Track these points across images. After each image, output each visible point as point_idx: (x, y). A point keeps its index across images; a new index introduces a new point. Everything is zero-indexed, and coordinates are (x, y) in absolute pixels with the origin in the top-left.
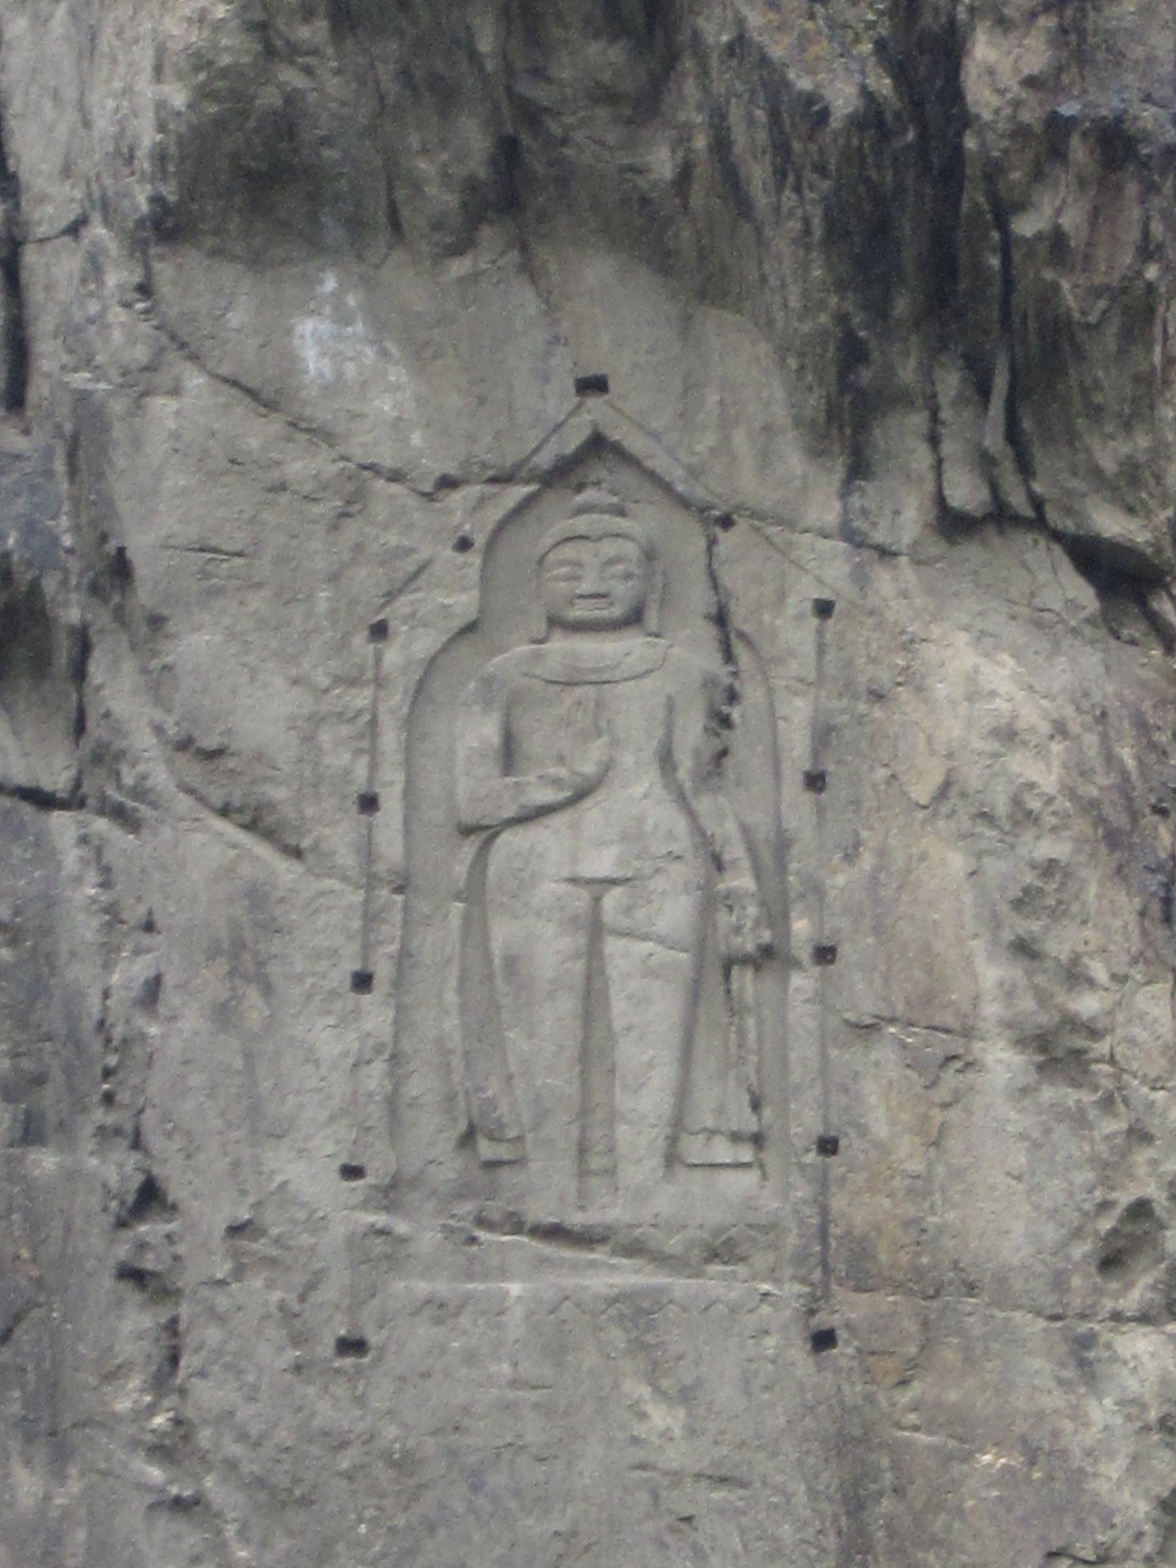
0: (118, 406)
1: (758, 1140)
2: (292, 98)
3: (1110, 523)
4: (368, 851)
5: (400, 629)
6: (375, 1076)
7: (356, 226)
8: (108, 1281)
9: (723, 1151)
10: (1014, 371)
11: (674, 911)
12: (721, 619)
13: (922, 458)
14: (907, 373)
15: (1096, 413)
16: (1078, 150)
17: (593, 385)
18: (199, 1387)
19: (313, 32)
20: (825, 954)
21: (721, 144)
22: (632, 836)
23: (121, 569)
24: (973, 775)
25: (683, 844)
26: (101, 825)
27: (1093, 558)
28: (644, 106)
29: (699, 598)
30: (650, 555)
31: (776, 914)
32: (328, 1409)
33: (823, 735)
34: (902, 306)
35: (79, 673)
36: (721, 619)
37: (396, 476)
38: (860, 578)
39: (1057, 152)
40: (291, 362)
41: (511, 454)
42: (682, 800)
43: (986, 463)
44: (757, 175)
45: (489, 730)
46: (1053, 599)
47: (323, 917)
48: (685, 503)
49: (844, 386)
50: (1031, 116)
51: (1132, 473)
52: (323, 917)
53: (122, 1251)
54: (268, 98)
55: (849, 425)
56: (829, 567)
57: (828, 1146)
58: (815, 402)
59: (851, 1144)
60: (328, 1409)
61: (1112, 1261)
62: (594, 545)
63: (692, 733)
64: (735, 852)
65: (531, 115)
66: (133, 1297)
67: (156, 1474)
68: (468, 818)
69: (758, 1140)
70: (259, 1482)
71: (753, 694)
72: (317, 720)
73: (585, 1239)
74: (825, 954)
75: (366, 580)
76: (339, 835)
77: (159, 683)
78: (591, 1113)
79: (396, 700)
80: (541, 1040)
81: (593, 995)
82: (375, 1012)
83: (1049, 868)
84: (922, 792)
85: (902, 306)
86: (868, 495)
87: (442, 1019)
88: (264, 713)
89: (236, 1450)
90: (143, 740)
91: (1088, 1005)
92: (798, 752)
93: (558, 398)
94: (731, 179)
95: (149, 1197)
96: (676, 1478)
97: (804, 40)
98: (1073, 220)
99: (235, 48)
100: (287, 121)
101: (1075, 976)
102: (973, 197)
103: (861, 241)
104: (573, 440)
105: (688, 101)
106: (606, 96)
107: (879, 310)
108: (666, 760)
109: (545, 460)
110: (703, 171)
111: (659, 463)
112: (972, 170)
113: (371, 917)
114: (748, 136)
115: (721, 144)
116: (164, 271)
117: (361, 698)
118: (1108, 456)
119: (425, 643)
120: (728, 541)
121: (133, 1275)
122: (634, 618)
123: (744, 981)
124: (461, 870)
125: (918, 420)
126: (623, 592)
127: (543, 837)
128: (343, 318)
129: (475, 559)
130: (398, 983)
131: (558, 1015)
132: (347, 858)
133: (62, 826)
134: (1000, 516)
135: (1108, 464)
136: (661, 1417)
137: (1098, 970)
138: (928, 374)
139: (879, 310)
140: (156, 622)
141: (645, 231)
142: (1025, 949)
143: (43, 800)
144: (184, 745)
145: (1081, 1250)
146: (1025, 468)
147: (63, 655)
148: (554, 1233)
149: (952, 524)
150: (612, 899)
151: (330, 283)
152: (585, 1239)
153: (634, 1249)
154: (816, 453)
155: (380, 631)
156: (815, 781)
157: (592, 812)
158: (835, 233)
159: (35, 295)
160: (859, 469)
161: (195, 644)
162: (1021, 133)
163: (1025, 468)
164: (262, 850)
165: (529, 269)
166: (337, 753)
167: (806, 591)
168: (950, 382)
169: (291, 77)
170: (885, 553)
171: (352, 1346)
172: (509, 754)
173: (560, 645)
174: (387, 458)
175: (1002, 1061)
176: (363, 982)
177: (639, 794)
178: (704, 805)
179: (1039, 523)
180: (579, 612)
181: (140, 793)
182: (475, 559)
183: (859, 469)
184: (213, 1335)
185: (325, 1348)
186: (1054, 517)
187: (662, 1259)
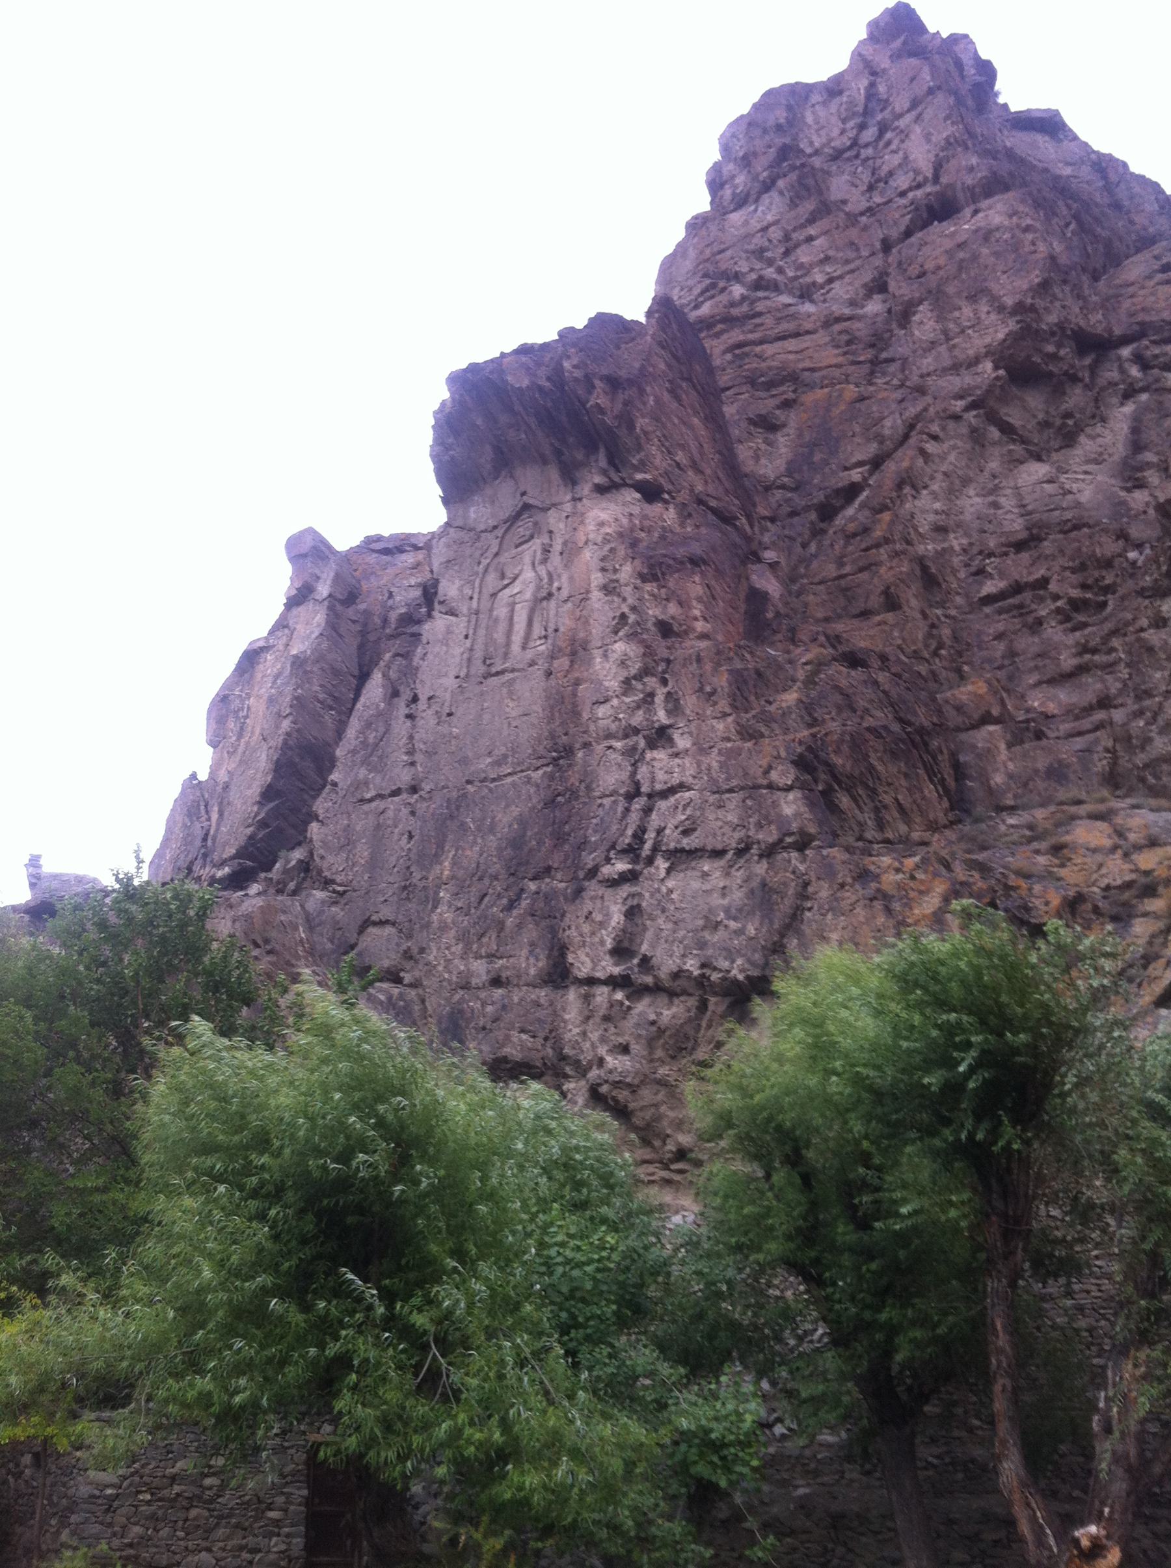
1: (546, 637)
3: (639, 476)
6: (466, 656)
8: (402, 719)
10: (607, 448)
11: (528, 595)
17: (523, 494)
20: (559, 589)
27: (640, 487)
32: (443, 729)
37: (485, 531)
38: (575, 507)
43: (604, 472)
46: (629, 499)
49: (560, 462)
51: (642, 462)
55: (570, 477)
56: (568, 507)
57: (556, 630)
60: (443, 729)
63: (539, 556)
69: (546, 637)
78: (508, 644)
81: (511, 619)
82: (468, 643)
85: (571, 440)
86: (578, 488)
108: (533, 564)
126: (528, 533)
127: (507, 592)
135: (635, 462)
142: (603, 570)
148: (497, 674)
153: (513, 670)
160: (574, 483)
165: (512, 477)
170: (580, 499)
171: (450, 715)
175: (596, 595)
176: (466, 637)
177: (528, 574)
179: (625, 485)
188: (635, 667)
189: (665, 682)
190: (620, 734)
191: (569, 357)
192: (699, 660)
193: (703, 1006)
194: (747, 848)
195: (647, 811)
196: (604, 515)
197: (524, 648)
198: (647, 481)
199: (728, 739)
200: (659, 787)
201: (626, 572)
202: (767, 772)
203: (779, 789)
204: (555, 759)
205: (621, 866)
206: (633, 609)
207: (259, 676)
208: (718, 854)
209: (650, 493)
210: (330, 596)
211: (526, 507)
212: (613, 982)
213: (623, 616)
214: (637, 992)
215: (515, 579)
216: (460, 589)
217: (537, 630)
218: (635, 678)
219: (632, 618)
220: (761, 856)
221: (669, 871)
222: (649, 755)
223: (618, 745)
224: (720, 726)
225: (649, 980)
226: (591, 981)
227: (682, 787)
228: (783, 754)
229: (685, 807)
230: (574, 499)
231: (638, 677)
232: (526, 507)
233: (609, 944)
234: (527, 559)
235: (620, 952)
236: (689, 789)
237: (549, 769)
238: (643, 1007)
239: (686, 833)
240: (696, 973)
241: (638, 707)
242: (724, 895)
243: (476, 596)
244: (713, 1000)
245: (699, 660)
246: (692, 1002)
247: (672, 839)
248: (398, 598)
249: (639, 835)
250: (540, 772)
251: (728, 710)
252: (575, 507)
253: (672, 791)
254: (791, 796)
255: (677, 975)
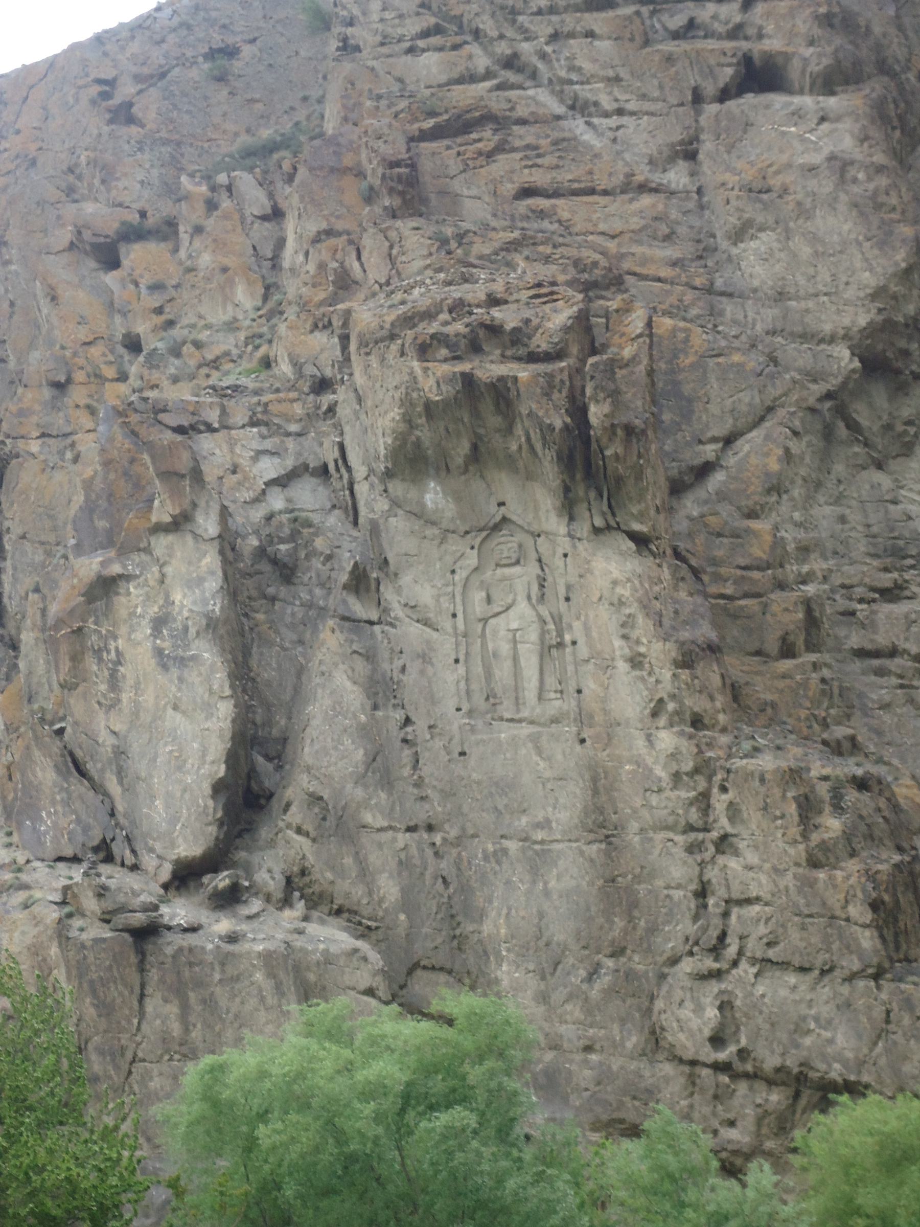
0: (381, 521)
1: (561, 692)
2: (418, 438)
3: (636, 527)
4: (455, 628)
5: (458, 571)
6: (462, 684)
7: (438, 469)
8: (398, 744)
9: (552, 695)
11: (534, 636)
12: (540, 561)
13: (587, 514)
14: (581, 493)
15: (630, 499)
16: (619, 432)
17: (501, 504)
18: (425, 768)
19: (422, 421)
21: (528, 439)
22: (522, 617)
23: (386, 561)
24: (606, 594)
25: (535, 619)
26: (387, 628)
28: (509, 430)
29: (534, 556)
30: (520, 546)
31: (560, 634)
33: (569, 587)
34: (579, 476)
35: (378, 590)
36: (540, 561)
37: (453, 532)
38: (574, 546)
39: (615, 434)
40: (423, 505)
41: (482, 524)
42: (534, 607)
43: (603, 514)
44: (538, 446)
45: (484, 594)
46: (624, 548)
47: (445, 646)
48: (528, 532)
49: (566, 497)
50: (607, 424)
52: (445, 646)
53: (402, 735)
54: (413, 438)
55: (569, 508)
56: (564, 544)
57: (579, 692)
58: (558, 504)
59: (586, 691)
61: (655, 714)
62: (505, 545)
64: (549, 619)
65: (478, 437)
66: (406, 746)
67: (416, 791)
68: (479, 616)
69: (561, 692)
70: (442, 791)
71: (550, 579)
72: (439, 596)
73: (520, 721)
74: (574, 643)
75: (449, 559)
76: (448, 624)
77: (399, 591)
79: (459, 589)
80: (503, 672)
81: (515, 659)
82: (461, 669)
83: (629, 615)
84: (595, 599)
85: (579, 476)
86: (575, 526)
87: (478, 670)
88: (425, 595)
89: (435, 783)
90: (395, 605)
91: (642, 649)
92: (562, 592)
93: (493, 508)
94: (532, 448)
95: (408, 721)
96: (548, 780)
97: (547, 410)
98: (620, 450)
99: (402, 427)
100: (418, 444)
101: (638, 642)
102: (594, 446)
103: (567, 461)
104: (498, 518)
105: (519, 430)
106: (499, 431)
107: (573, 477)
108: (529, 598)
109: (491, 524)
110: (525, 446)
111: (520, 522)
112: (593, 440)
113: (457, 644)
114: (536, 437)
115: (528, 439)
116: (390, 486)
117: (450, 589)
118: (634, 510)
119: (464, 574)
120: (540, 540)
121: (405, 741)
122: (518, 562)
123: (554, 652)
124: (479, 630)
125: (585, 505)
126: (514, 557)
127: (500, 621)
128: (436, 493)
129: (475, 551)
130: (466, 661)
131: (508, 664)
132: (450, 630)
133: (377, 628)
134: (609, 527)
136: (542, 764)
137: (644, 640)
138: (586, 493)
139: (573, 477)
140: (396, 575)
141: (510, 463)
142: (625, 637)
143: (371, 623)
144: (406, 605)
145: (648, 711)
146: (614, 515)
147: (373, 586)
148: (511, 720)
149: (596, 531)
150: (518, 634)
151: (432, 485)
152: (520, 721)
153: (532, 722)
154: (560, 515)
155: (453, 572)
156: (568, 599)
157: (511, 612)
158: (560, 458)
159: (358, 496)
161: (406, 579)
162: (605, 429)
163: (614, 515)
164: (428, 630)
166: (445, 604)
167: (560, 551)
168: (592, 494)
169: (418, 433)
171: (463, 754)
172: (489, 600)
173: (499, 571)
174: (452, 528)
175: (622, 666)
176: (457, 661)
177: (522, 606)
178: (540, 608)
179: (619, 528)
180: (504, 562)
181: (396, 618)
182: (475, 551)
183: (572, 519)
184: (427, 754)
185: (456, 755)
186: (623, 527)
187: (539, 724)
188: (688, 766)
189: (724, 789)
190: (680, 828)
191: (597, 401)
192: (762, 780)
193: (797, 1095)
194: (831, 970)
195: (726, 915)
196: (612, 568)
197: (540, 698)
198: (642, 533)
199: (797, 864)
200: (736, 895)
201: (659, 652)
202: (844, 908)
203: (856, 924)
204: (607, 837)
205: (710, 963)
206: (673, 697)
207: (123, 613)
208: (803, 970)
209: (641, 541)
210: (220, 536)
211: (505, 519)
212: (720, 1067)
213: (661, 701)
214: (736, 1076)
215: (508, 609)
216: (437, 599)
217: (551, 681)
218: (687, 774)
219: (671, 706)
220: (844, 980)
221: (757, 975)
222: (721, 860)
223: (680, 839)
224: (792, 851)
225: (749, 1068)
226: (693, 1063)
227: (758, 899)
228: (860, 895)
229: (768, 920)
230: (570, 535)
231: (691, 774)
232: (505, 519)
233: (707, 1033)
234: (520, 587)
235: (717, 1041)
236: (767, 904)
237: (603, 846)
238: (742, 1087)
239: (769, 944)
240: (796, 1070)
241: (691, 804)
242: (810, 1007)
243: (460, 616)
244: (808, 1092)
245: (762, 780)
246: (790, 1091)
247: (754, 947)
248: (239, 520)
249: (722, 937)
250: (595, 847)
251: (799, 839)
252: (574, 546)
253: (748, 901)
254: (867, 933)
255: (778, 1070)
